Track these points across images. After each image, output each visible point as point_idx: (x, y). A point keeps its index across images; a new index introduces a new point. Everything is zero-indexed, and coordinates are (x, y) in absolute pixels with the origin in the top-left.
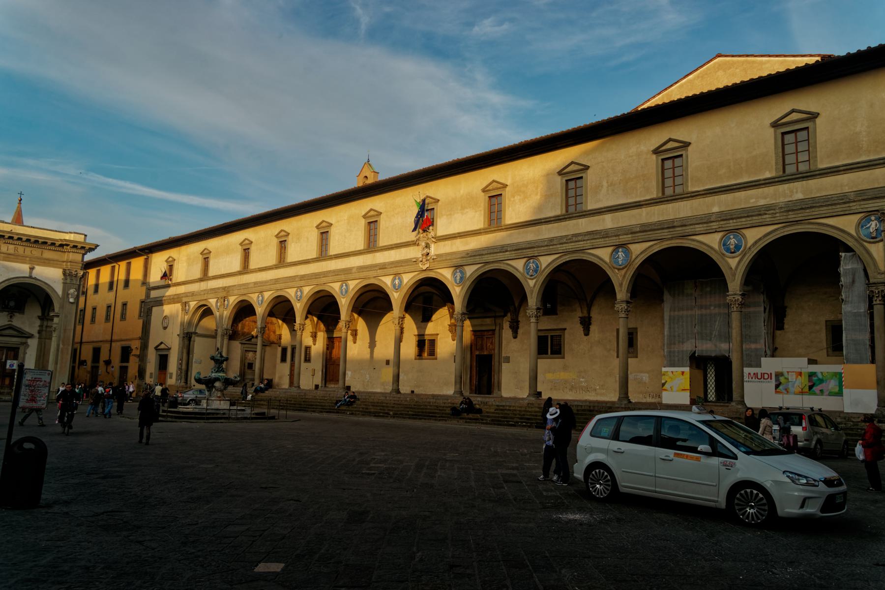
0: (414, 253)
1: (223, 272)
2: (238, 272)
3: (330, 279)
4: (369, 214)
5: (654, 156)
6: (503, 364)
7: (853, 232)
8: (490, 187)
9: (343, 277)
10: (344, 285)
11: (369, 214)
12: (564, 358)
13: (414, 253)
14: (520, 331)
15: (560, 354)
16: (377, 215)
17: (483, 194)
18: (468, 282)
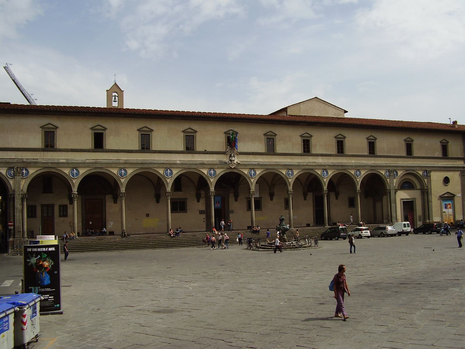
0: (225, 159)
1: (14, 145)
2: (41, 149)
3: (156, 165)
4: (188, 130)
5: (335, 139)
6: (230, 214)
7: (384, 174)
8: (268, 134)
9: (168, 166)
10: (169, 170)
11: (188, 130)
12: (262, 210)
13: (225, 159)
14: (239, 198)
15: (260, 208)
16: (194, 132)
17: (264, 136)
18: (258, 177)
